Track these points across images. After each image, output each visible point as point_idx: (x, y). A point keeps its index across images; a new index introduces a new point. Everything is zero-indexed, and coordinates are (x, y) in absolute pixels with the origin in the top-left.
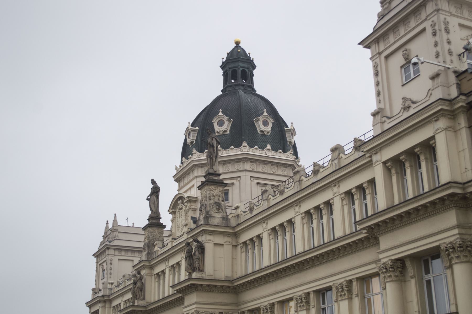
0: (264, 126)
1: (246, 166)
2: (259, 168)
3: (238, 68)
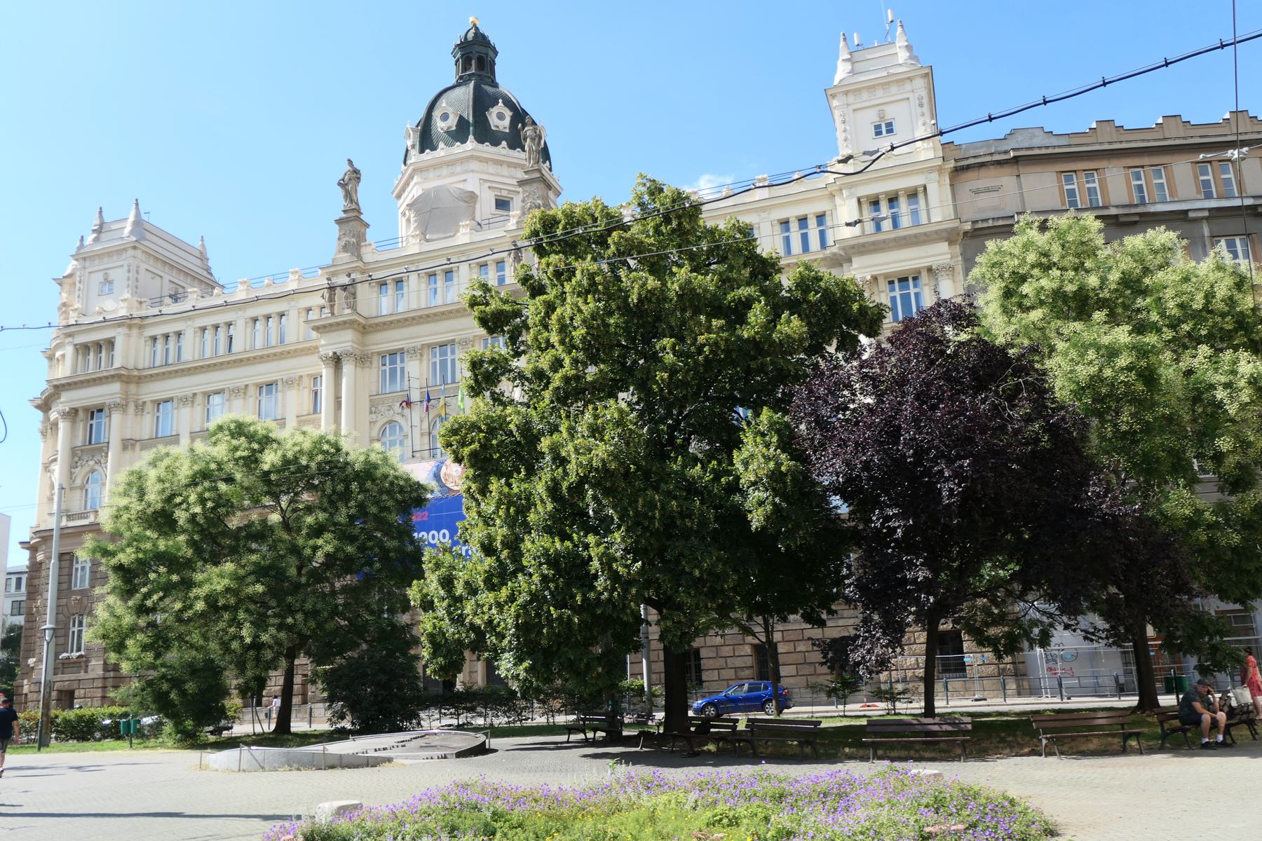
0: (499, 119)
1: (474, 165)
2: (492, 168)
3: (476, 56)
